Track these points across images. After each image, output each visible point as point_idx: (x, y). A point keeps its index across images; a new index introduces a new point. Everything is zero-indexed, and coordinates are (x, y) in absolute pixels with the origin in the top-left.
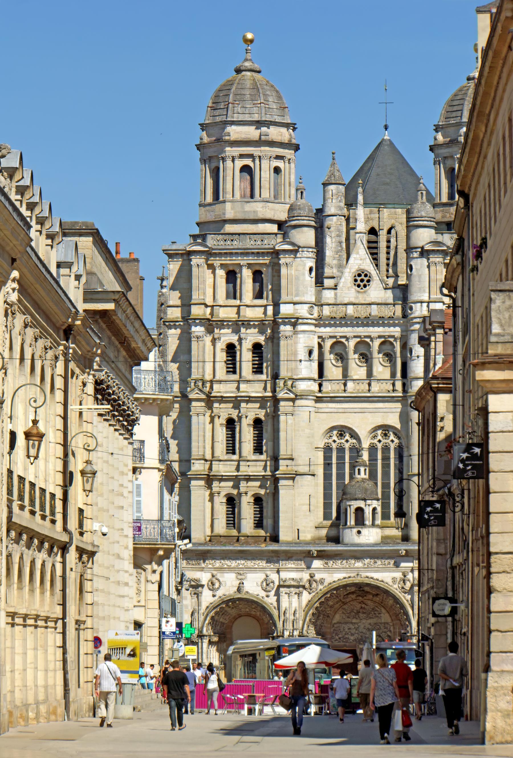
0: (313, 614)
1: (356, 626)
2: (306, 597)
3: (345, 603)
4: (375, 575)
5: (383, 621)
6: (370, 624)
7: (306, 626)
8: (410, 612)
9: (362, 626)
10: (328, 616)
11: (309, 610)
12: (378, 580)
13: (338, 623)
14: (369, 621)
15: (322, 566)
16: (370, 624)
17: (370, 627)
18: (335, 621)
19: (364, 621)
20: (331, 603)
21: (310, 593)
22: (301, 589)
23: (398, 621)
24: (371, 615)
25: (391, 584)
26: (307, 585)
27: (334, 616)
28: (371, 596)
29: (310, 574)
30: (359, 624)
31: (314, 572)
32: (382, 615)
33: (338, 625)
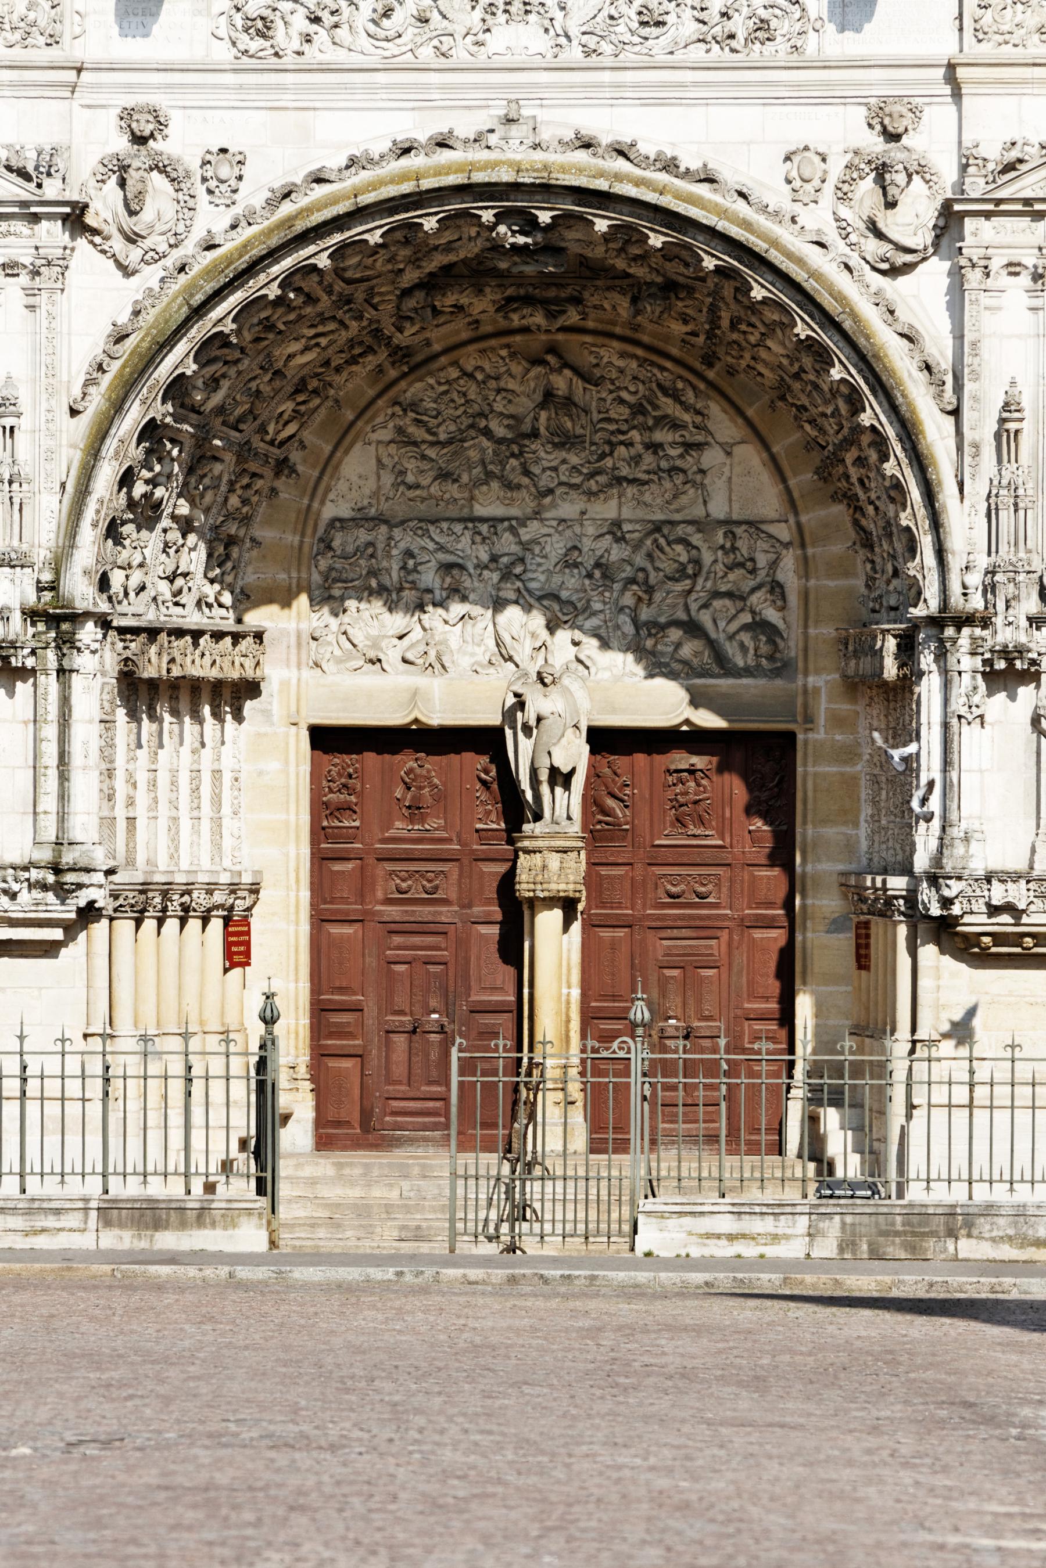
0: (151, 432)
1: (507, 544)
2: (99, 300)
3: (412, 362)
4: (654, 131)
5: (718, 509)
6: (615, 530)
7: (88, 536)
8: (937, 433)
9: (556, 547)
10: (283, 466)
11: (117, 406)
12: (670, 165)
13: (361, 519)
14: (607, 509)
15: (224, 53)
16: (615, 530)
17: (617, 553)
18: (336, 507)
19: (568, 508)
20: (297, 355)
21: (127, 272)
22: (52, 234)
23: (839, 510)
24: (619, 460)
25: (778, 197)
26: (105, 205)
27: (329, 465)
28: (624, 306)
29: (128, 114)
30: (531, 531)
31: (159, 100)
32: (712, 457)
33: (363, 536)
